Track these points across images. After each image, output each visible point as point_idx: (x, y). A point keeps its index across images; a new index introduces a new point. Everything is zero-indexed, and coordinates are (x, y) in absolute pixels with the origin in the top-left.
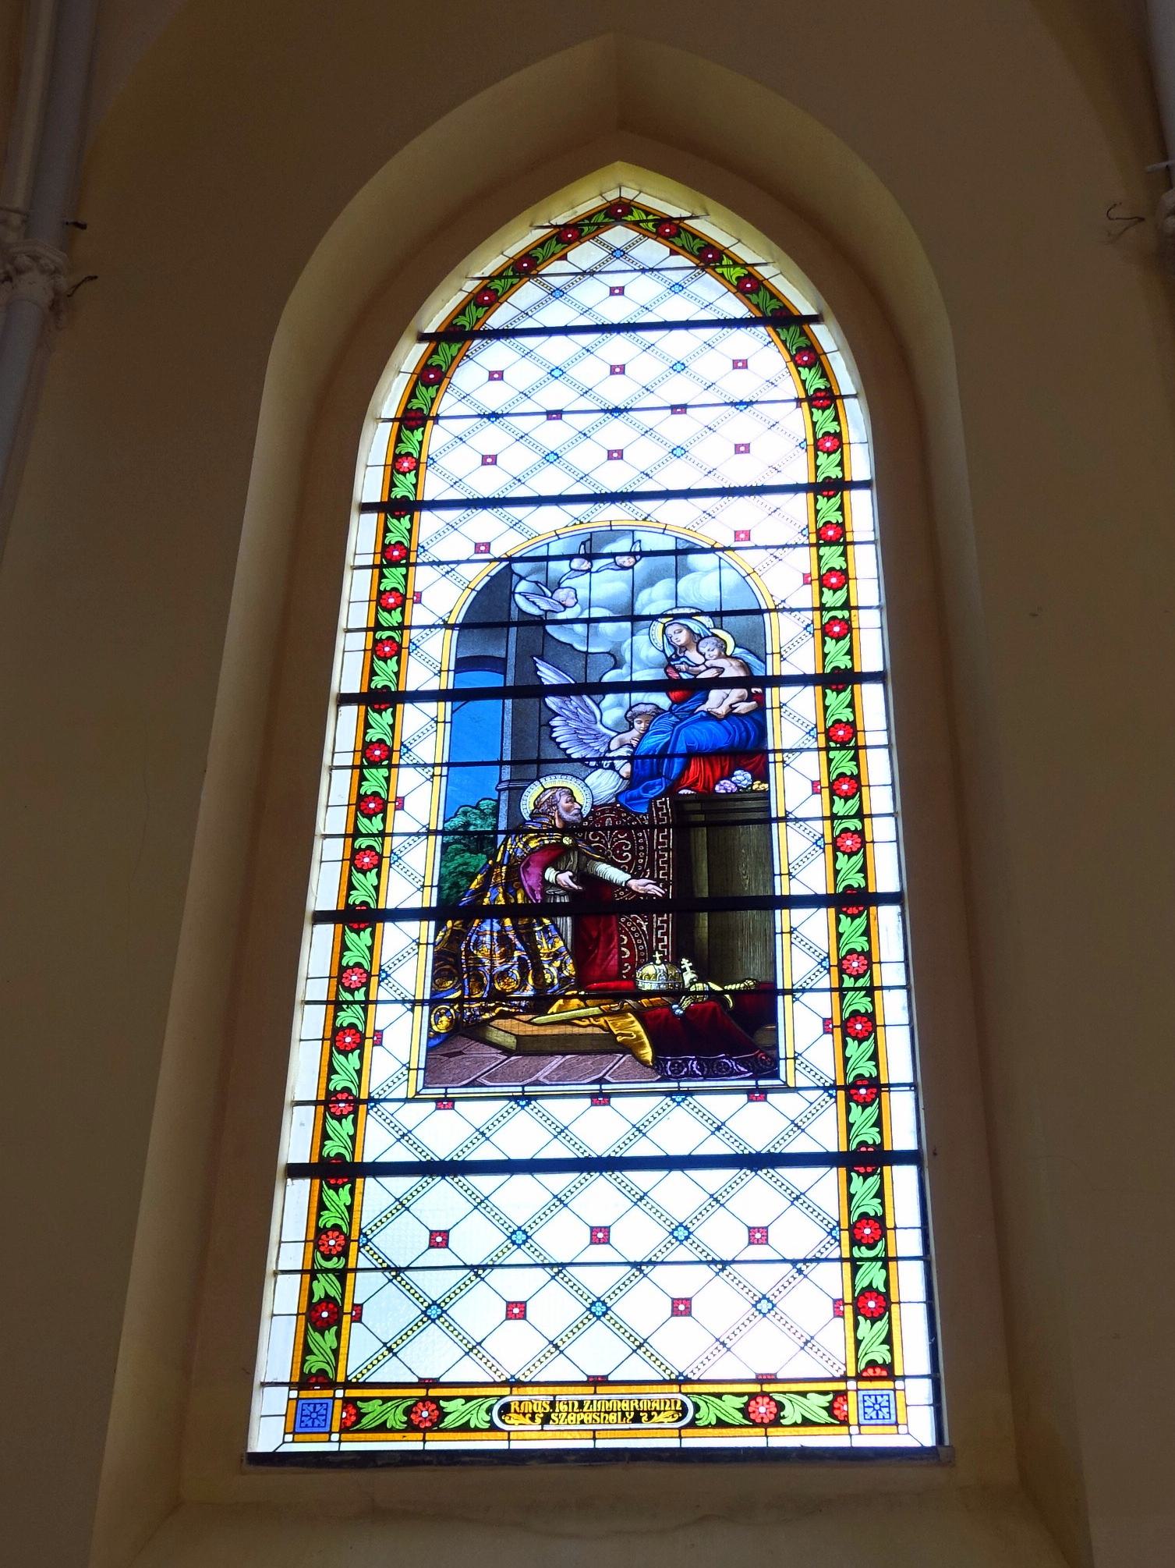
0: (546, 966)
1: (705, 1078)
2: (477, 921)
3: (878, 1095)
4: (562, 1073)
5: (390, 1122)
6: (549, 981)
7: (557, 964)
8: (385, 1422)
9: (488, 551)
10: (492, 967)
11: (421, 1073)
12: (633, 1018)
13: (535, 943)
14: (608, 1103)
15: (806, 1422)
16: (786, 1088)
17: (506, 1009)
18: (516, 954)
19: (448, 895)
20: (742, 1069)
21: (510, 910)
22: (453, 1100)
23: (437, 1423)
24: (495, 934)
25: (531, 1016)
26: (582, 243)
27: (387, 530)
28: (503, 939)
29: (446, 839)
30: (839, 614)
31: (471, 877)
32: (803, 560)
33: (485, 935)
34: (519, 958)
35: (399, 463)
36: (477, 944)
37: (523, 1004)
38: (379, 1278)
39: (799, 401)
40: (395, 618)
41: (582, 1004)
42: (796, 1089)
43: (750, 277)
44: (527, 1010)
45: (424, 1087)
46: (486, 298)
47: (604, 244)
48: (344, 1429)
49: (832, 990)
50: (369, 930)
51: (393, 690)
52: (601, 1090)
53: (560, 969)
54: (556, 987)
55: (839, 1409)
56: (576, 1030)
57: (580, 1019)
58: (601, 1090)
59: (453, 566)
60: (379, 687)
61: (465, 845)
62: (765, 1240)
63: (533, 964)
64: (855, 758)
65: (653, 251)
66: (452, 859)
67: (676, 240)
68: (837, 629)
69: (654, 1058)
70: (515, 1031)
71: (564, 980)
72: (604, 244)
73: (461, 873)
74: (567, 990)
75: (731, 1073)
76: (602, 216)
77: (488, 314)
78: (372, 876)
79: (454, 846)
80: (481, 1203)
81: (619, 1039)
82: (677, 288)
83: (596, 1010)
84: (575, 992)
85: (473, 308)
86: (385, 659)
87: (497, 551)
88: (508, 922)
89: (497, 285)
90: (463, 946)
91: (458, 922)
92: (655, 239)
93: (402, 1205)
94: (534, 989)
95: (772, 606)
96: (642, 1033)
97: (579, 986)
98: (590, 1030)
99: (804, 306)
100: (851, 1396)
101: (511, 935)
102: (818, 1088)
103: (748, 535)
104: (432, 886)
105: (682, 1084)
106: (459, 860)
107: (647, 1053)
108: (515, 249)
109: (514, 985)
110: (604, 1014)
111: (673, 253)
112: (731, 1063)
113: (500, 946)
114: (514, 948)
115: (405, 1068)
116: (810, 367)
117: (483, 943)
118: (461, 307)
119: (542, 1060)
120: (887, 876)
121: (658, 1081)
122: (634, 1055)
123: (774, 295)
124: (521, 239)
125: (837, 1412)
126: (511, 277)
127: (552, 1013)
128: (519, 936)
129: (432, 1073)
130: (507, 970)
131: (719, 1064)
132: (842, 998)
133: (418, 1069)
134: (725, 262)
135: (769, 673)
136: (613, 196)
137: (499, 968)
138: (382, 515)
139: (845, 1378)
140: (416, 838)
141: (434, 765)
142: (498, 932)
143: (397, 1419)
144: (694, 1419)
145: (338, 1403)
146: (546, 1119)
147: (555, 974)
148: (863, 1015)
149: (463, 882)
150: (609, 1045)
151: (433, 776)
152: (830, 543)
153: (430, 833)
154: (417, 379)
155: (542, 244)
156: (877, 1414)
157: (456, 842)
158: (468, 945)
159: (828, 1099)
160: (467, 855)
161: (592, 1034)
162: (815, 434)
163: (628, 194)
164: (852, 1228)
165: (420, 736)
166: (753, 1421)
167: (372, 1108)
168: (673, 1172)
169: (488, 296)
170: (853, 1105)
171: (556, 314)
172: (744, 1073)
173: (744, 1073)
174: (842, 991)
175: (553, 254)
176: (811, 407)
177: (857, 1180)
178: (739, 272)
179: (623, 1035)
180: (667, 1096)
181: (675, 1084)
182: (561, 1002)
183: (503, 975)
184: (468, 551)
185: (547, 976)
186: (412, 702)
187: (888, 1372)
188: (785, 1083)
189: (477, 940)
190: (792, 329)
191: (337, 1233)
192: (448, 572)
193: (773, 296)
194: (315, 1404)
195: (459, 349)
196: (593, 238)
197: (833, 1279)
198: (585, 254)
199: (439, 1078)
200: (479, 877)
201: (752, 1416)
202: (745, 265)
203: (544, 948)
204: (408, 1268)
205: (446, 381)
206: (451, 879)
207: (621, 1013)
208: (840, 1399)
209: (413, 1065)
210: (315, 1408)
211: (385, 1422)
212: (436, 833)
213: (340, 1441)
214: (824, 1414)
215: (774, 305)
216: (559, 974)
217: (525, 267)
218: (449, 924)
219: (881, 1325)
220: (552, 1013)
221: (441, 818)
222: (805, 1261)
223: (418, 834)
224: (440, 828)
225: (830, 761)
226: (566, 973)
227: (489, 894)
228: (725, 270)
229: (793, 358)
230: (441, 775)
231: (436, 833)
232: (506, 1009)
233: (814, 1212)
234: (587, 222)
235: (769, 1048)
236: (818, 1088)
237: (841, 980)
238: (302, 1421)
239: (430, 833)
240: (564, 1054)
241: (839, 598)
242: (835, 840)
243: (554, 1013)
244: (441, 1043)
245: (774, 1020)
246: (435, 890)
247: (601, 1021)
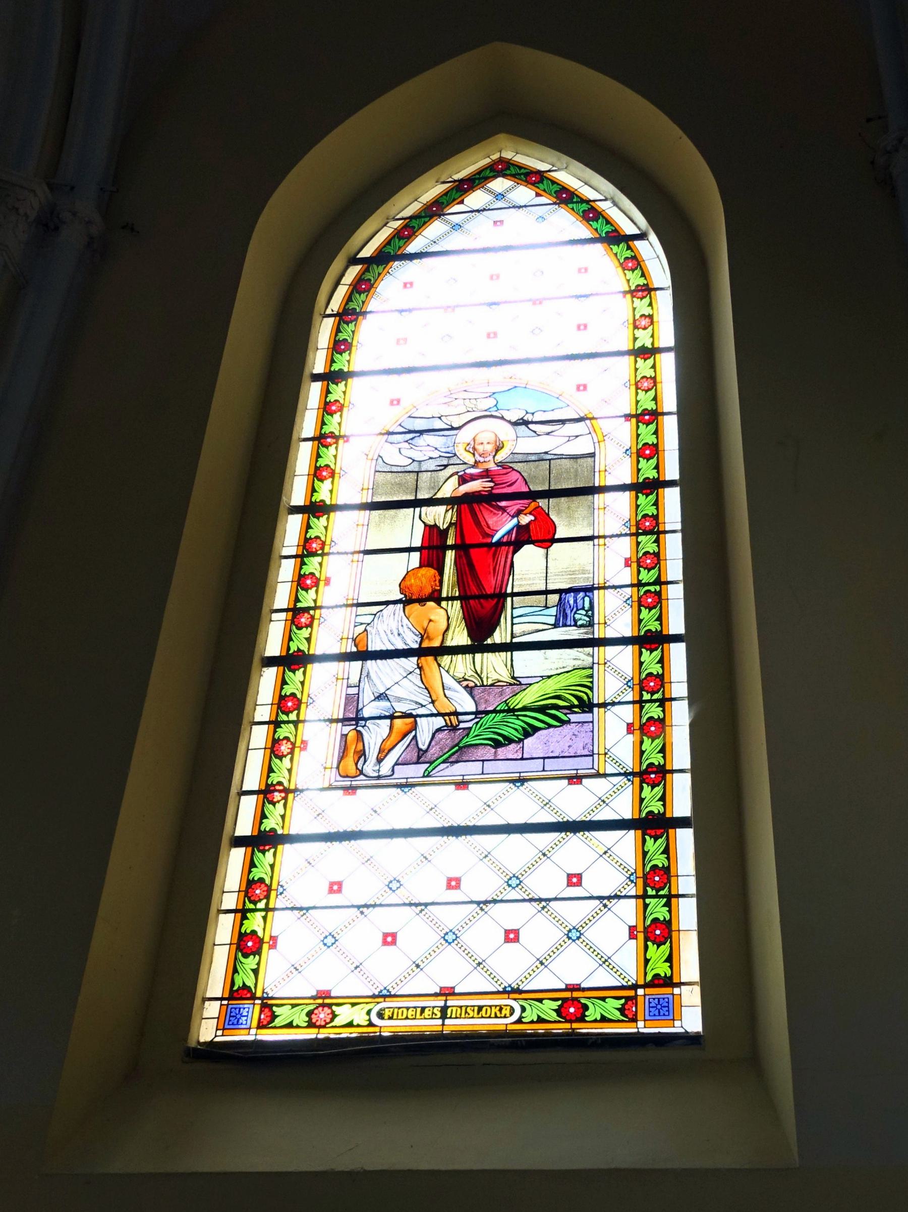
3: (664, 778)
26: (474, 191)
42: (605, 775)
43: (593, 209)
47: (490, 192)
49: (634, 702)
62: (579, 884)
64: (657, 541)
65: (524, 194)
67: (541, 186)
68: (648, 452)
72: (490, 192)
99: (629, 229)
100: (640, 1000)
102: (620, 774)
111: (538, 195)
116: (633, 270)
120: (676, 624)
132: (642, 708)
148: (656, 720)
159: (627, 782)
163: (508, 155)
169: (409, 230)
176: (633, 296)
177: (650, 841)
178: (584, 207)
188: (598, 771)
193: (608, 222)
197: (628, 911)
202: (588, 201)
215: (608, 228)
219: (665, 948)
222: (609, 898)
225: (638, 544)
228: (574, 205)
236: (620, 774)
237: (641, 695)
242: (639, 599)
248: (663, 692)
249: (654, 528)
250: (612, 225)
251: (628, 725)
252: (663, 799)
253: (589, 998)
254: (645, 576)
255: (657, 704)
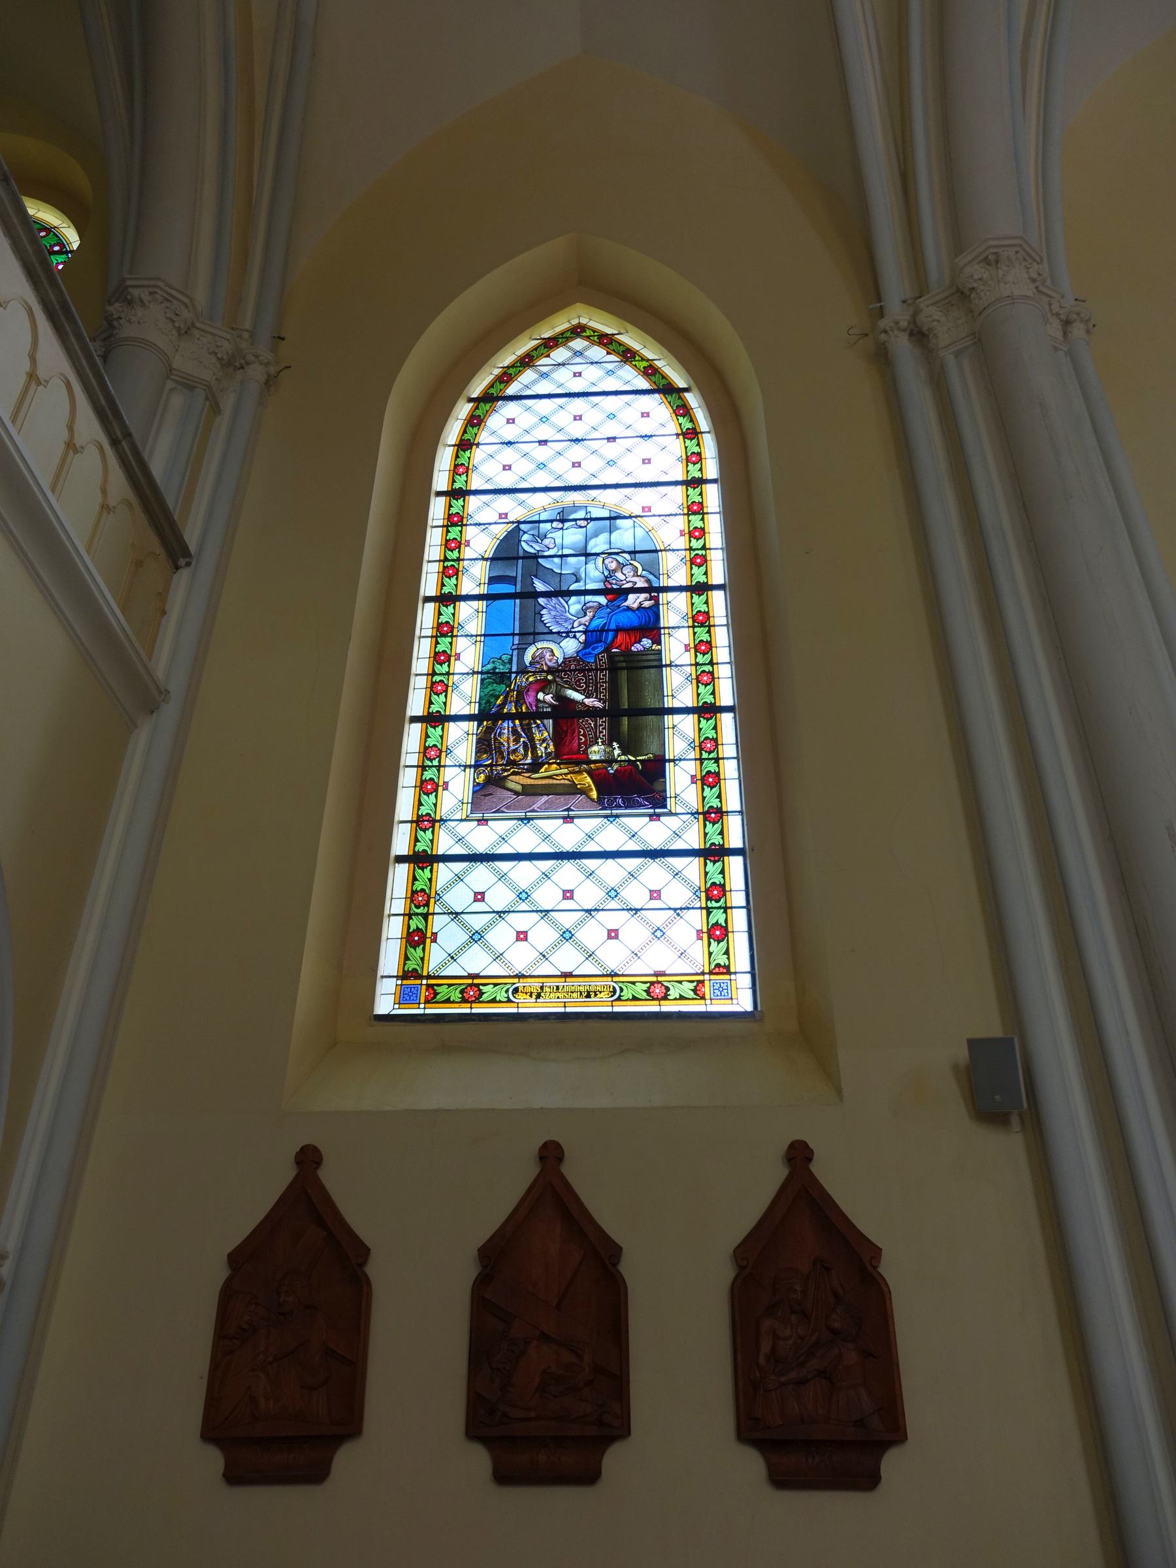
0: (538, 746)
1: (626, 808)
2: (500, 722)
4: (547, 805)
5: (452, 832)
6: (540, 754)
7: (544, 745)
8: (449, 998)
9: (506, 518)
10: (509, 747)
11: (469, 805)
12: (586, 775)
13: (533, 734)
15: (682, 998)
16: (671, 814)
17: (516, 770)
18: (522, 740)
19: (484, 707)
20: (646, 803)
21: (519, 716)
22: (487, 820)
23: (478, 998)
24: (510, 729)
25: (530, 774)
27: (450, 506)
28: (514, 731)
29: (483, 676)
30: (700, 552)
31: (497, 697)
32: (680, 523)
33: (504, 729)
34: (524, 742)
35: (458, 469)
36: (500, 734)
37: (526, 767)
38: (447, 918)
39: (678, 435)
40: (455, 555)
41: (558, 767)
42: (676, 814)
43: (651, 367)
44: (528, 771)
45: (471, 813)
46: (505, 378)
47: (570, 349)
48: (427, 1001)
49: (696, 759)
50: (441, 726)
51: (454, 594)
52: (569, 814)
53: (546, 748)
54: (544, 758)
55: (700, 990)
56: (555, 782)
57: (557, 775)
58: (569, 814)
59: (487, 526)
60: (446, 592)
61: (493, 680)
62: (659, 897)
63: (531, 745)
64: (709, 632)
65: (597, 352)
66: (487, 688)
67: (610, 346)
68: (698, 561)
69: (598, 797)
70: (521, 782)
71: (548, 755)
72: (570, 349)
73: (491, 695)
74: (550, 759)
75: (641, 806)
76: (569, 333)
77: (506, 387)
78: (442, 697)
79: (487, 680)
80: (502, 877)
81: (579, 786)
82: (610, 373)
83: (566, 771)
84: (554, 761)
85: (498, 384)
86: (449, 577)
87: (511, 518)
88: (517, 722)
89: (511, 371)
90: (493, 735)
91: (490, 722)
92: (598, 346)
93: (459, 878)
94: (532, 759)
95: (663, 548)
96: (591, 783)
97: (556, 757)
98: (562, 782)
99: (681, 383)
100: (707, 983)
101: (519, 729)
102: (688, 813)
103: (649, 509)
104: (475, 702)
105: (613, 811)
106: (490, 688)
107: (594, 794)
108: (521, 352)
109: (521, 757)
110: (570, 773)
111: (608, 353)
112: (640, 800)
113: (513, 735)
114: (521, 736)
117: (503, 734)
118: (491, 383)
120: (726, 697)
121: (600, 810)
122: (587, 796)
123: (664, 377)
124: (524, 345)
125: (699, 992)
126: (519, 367)
127: (542, 772)
128: (523, 730)
129: (476, 805)
130: (517, 749)
131: (634, 801)
132: (701, 764)
133: (468, 803)
134: (637, 359)
135: (661, 585)
136: (575, 322)
137: (512, 748)
138: (448, 498)
139: (703, 973)
140: (467, 676)
141: (476, 636)
142: (512, 728)
143: (456, 995)
144: (620, 996)
145: (424, 987)
146: (539, 831)
147: (543, 751)
148: (713, 773)
149: (492, 700)
150: (573, 790)
151: (476, 641)
152: (695, 513)
153: (474, 673)
154: (467, 423)
155: (536, 349)
156: (721, 993)
157: (488, 678)
158: (495, 735)
159: (694, 819)
160: (495, 685)
161: (564, 784)
162: (686, 453)
163: (584, 321)
164: (707, 891)
165: (468, 620)
166: (652, 997)
167: (442, 824)
168: (608, 860)
169: (506, 377)
170: (707, 823)
171: (544, 387)
172: (648, 805)
173: (648, 805)
174: (701, 760)
175: (542, 354)
176: (684, 438)
177: (710, 864)
178: (645, 364)
179: (581, 784)
180: (605, 818)
181: (609, 812)
182: (546, 766)
183: (515, 751)
184: (495, 518)
185: (539, 752)
186: (464, 601)
187: (727, 970)
188: (670, 811)
189: (500, 732)
190: (674, 395)
191: (423, 894)
192: (484, 529)
193: (663, 377)
194: (411, 988)
195: (491, 406)
196: (564, 345)
197: (696, 919)
198: (560, 354)
199: (479, 808)
200: (501, 697)
201: (652, 994)
202: (648, 360)
203: (537, 736)
204: (462, 913)
205: (483, 424)
206: (486, 698)
207: (580, 772)
208: (700, 985)
209: (465, 801)
210: (411, 990)
211: (449, 998)
212: (478, 673)
213: (425, 1008)
214: (692, 993)
215: (664, 382)
216: (545, 751)
217: (527, 361)
218: (485, 723)
220: (542, 772)
221: (480, 665)
222: (681, 909)
223: (468, 674)
224: (480, 670)
225: (695, 633)
226: (549, 750)
227: (507, 707)
228: (637, 363)
229: (674, 411)
230: (480, 641)
231: (478, 673)
232: (516, 770)
233: (686, 882)
234: (561, 336)
235: (661, 792)
237: (701, 754)
238: (404, 997)
239: (474, 673)
240: (548, 795)
241: (700, 543)
243: (543, 771)
244: (479, 789)
245: (664, 776)
246: (477, 704)
247: (569, 777)
248: (718, 752)
249: (706, 622)
250: (666, 379)
251: (692, 776)
252: (721, 833)
253: (670, 981)
254: (700, 659)
255: (713, 761)
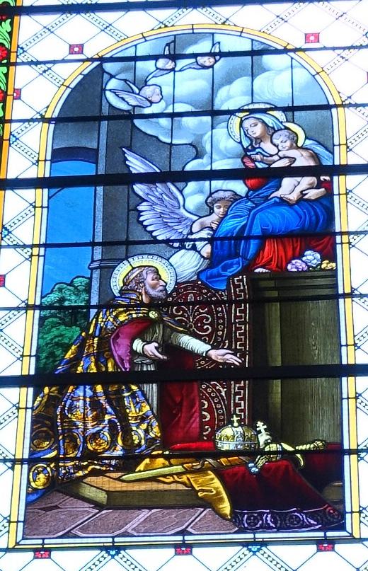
0: (134, 428)
1: (279, 530)
2: (71, 387)
4: (148, 526)
6: (137, 442)
7: (144, 426)
10: (85, 429)
11: (21, 525)
12: (213, 476)
13: (124, 407)
14: (191, 553)
17: (98, 467)
18: (107, 417)
19: (45, 364)
20: (312, 522)
21: (102, 378)
22: (49, 550)
24: (88, 400)
25: (120, 474)
28: (95, 404)
29: (43, 313)
31: (66, 348)
33: (78, 400)
34: (110, 421)
36: (71, 409)
37: (113, 462)
41: (167, 463)
44: (117, 469)
45: (23, 538)
52: (184, 540)
53: (146, 431)
54: (143, 448)
56: (161, 486)
57: (165, 476)
58: (184, 540)
61: (60, 318)
63: (122, 427)
66: (49, 331)
69: (232, 512)
70: (106, 488)
71: (150, 442)
73: (57, 344)
74: (153, 450)
75: (302, 526)
79: (50, 320)
81: (200, 494)
83: (179, 469)
84: (160, 452)
88: (99, 388)
90: (59, 410)
91: (54, 389)
94: (123, 449)
96: (221, 489)
97: (163, 447)
98: (173, 486)
101: (103, 400)
104: (30, 356)
105: (258, 536)
106: (55, 332)
107: (226, 507)
109: (105, 446)
110: (187, 472)
112: (302, 517)
113: (92, 410)
114: (105, 412)
115: (6, 521)
117: (77, 407)
119: (130, 513)
121: (236, 532)
122: (214, 509)
127: (140, 471)
128: (109, 402)
129: (31, 524)
130: (98, 432)
131: (291, 517)
133: (18, 522)
137: (91, 430)
140: (16, 313)
141: (32, 246)
142: (90, 398)
147: (142, 436)
149: (59, 352)
150: (192, 500)
151: (31, 256)
153: (28, 307)
157: (52, 316)
158: (63, 409)
160: (63, 327)
161: (176, 490)
165: (19, 220)
172: (314, 525)
173: (314, 525)
179: (203, 491)
180: (244, 546)
181: (251, 536)
182: (147, 461)
183: (95, 436)
185: (135, 437)
186: (12, 189)
189: (71, 405)
199: (36, 529)
200: (73, 347)
203: (132, 412)
206: (48, 350)
207: (202, 471)
209: (14, 518)
212: (34, 307)
216: (145, 436)
218: (46, 390)
220: (140, 471)
221: (39, 294)
223: (18, 309)
224: (38, 303)
226: (152, 435)
227: (82, 363)
230: (38, 255)
231: (34, 307)
232: (98, 467)
235: (336, 503)
239: (28, 307)
240: (150, 508)
243: (142, 470)
244: (35, 500)
245: (341, 478)
246: (33, 359)
247: (184, 478)
